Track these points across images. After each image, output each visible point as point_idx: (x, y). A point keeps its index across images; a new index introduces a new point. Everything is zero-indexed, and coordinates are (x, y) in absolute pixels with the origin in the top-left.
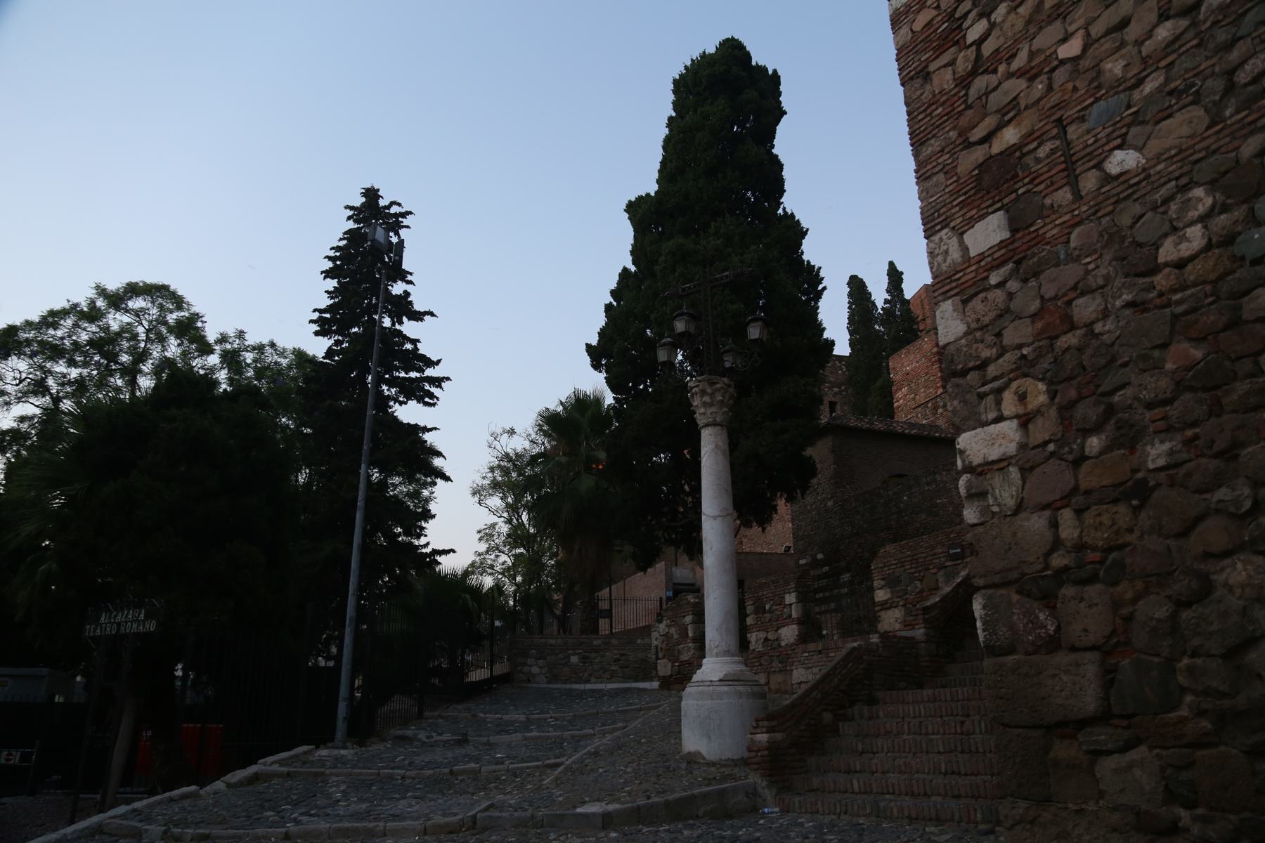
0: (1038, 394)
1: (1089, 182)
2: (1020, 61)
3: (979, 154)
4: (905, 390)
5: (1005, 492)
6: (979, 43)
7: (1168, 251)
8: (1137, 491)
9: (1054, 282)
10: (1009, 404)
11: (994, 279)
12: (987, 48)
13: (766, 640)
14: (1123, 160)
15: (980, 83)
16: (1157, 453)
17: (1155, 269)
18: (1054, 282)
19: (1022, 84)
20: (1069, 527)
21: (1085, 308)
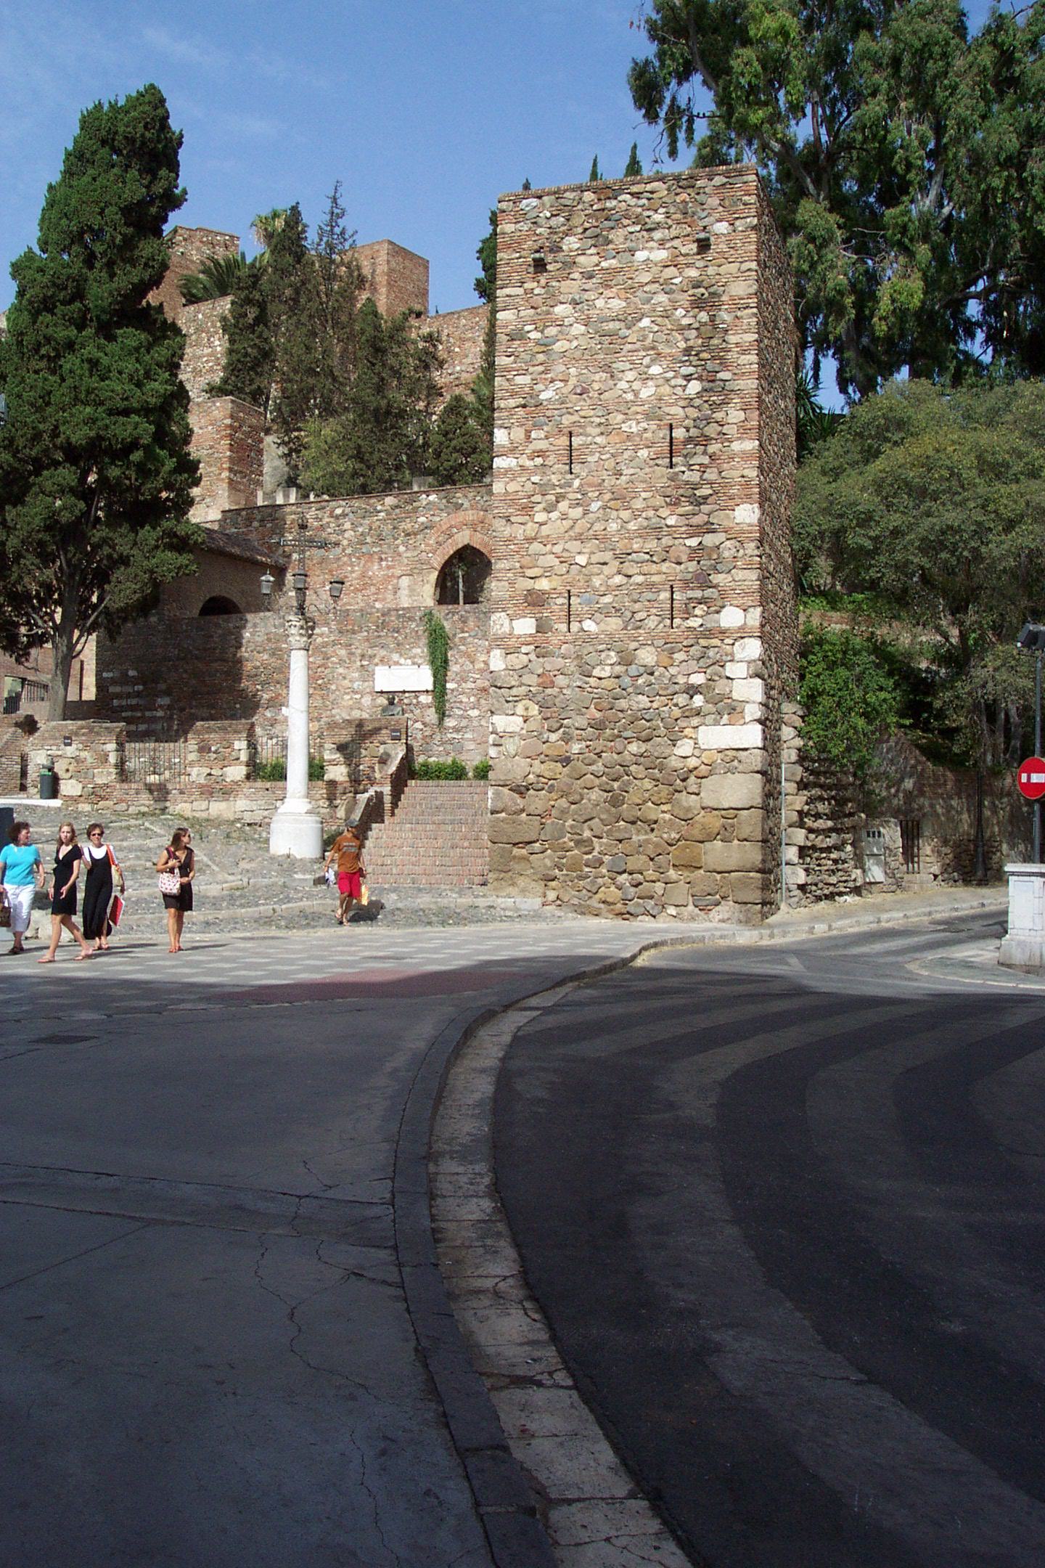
0: (534, 710)
1: (575, 626)
2: (558, 549)
3: (529, 584)
5: (511, 746)
6: (541, 524)
7: (596, 672)
8: (566, 761)
10: (520, 709)
11: (524, 649)
12: (545, 530)
13: (210, 774)
14: (589, 625)
15: (536, 547)
16: (576, 747)
20: (538, 767)
21: (561, 681)
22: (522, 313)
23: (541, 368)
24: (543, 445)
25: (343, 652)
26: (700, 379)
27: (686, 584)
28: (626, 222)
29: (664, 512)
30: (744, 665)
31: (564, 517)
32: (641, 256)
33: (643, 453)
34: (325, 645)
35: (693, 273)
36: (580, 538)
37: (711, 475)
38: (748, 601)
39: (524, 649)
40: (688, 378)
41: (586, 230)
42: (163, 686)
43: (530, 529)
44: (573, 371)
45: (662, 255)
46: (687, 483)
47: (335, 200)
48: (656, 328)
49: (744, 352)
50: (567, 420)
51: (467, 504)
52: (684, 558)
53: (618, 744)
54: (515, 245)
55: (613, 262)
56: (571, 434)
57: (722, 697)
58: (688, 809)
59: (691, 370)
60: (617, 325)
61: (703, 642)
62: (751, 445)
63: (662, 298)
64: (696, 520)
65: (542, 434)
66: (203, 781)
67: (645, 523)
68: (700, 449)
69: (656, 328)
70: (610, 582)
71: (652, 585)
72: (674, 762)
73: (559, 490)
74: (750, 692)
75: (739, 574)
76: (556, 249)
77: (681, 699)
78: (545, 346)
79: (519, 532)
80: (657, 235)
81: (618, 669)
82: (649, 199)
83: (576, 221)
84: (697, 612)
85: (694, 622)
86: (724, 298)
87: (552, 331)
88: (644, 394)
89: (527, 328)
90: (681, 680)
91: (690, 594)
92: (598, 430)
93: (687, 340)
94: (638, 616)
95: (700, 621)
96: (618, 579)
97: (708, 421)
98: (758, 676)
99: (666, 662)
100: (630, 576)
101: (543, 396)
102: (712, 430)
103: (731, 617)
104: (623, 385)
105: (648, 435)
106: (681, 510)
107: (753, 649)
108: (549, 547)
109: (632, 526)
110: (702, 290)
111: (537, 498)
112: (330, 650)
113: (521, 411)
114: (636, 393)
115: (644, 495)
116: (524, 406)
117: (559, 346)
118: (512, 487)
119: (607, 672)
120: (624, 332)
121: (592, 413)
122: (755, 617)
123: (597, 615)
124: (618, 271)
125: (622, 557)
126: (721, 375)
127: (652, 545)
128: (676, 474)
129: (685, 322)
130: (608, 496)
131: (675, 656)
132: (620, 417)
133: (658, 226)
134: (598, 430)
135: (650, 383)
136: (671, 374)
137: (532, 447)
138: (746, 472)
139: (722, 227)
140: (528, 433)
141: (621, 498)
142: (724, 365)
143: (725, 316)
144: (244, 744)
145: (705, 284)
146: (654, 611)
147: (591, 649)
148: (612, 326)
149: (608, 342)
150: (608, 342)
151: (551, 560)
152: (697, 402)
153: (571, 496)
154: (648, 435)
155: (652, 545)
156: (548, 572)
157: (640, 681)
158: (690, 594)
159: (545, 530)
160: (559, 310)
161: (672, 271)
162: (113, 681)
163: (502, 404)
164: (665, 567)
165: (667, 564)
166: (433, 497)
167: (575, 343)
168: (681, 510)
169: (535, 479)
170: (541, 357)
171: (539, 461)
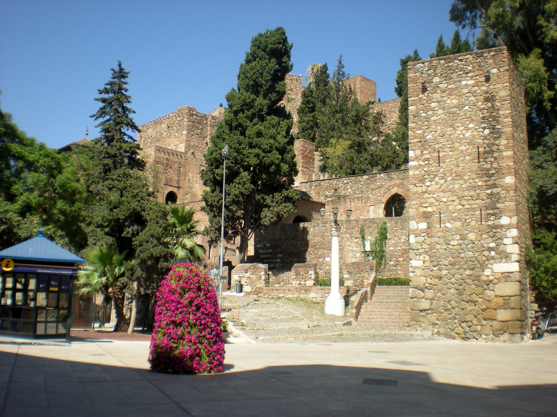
0: (427, 258)
1: (443, 225)
2: (435, 196)
3: (424, 210)
5: (418, 272)
6: (428, 186)
7: (452, 243)
8: (440, 278)
9: (433, 240)
11: (423, 235)
12: (430, 189)
13: (300, 284)
14: (448, 225)
15: (426, 195)
16: (444, 272)
17: (449, 244)
18: (433, 240)
19: (435, 201)
20: (429, 281)
22: (418, 107)
23: (426, 127)
24: (428, 156)
25: (349, 236)
26: (489, 128)
27: (487, 208)
28: (457, 70)
29: (476, 180)
30: (511, 239)
31: (437, 183)
32: (464, 83)
33: (468, 158)
35: (484, 88)
36: (443, 191)
37: (495, 165)
38: (512, 214)
39: (423, 235)
40: (484, 128)
41: (442, 74)
42: (279, 250)
43: (424, 189)
44: (439, 127)
45: (471, 82)
46: (485, 169)
47: (340, 62)
48: (471, 110)
49: (506, 117)
50: (437, 146)
52: (485, 198)
53: (461, 271)
54: (415, 81)
55: (453, 85)
56: (439, 152)
57: (503, 252)
58: (490, 297)
59: (485, 125)
60: (456, 109)
61: (494, 230)
62: (510, 153)
63: (472, 98)
64: (489, 183)
65: (427, 152)
66: (297, 286)
67: (469, 185)
68: (490, 155)
69: (471, 110)
70: (456, 208)
71: (473, 208)
72: (484, 278)
73: (435, 173)
74: (514, 250)
75: (507, 204)
76: (431, 82)
77: (486, 253)
78: (428, 119)
79: (420, 190)
80: (470, 75)
81: (460, 242)
82: (466, 62)
83: (439, 71)
84: (492, 219)
85: (490, 223)
86: (497, 97)
87: (430, 113)
88: (467, 135)
89: (421, 112)
90: (485, 245)
91: (488, 212)
92: (450, 150)
93: (483, 114)
94: (468, 221)
95: (492, 222)
96: (459, 207)
97: (493, 144)
98: (516, 243)
99: (479, 238)
100: (463, 206)
101: (427, 138)
102: (494, 148)
103: (505, 220)
104: (458, 132)
105: (469, 151)
106: (483, 179)
107: (514, 232)
108: (432, 195)
109: (464, 186)
110: (488, 95)
111: (426, 177)
113: (419, 144)
114: (464, 135)
115: (468, 174)
116: (420, 142)
117: (433, 118)
118: (417, 172)
119: (455, 243)
120: (458, 112)
121: (447, 143)
122: (514, 220)
123: (451, 221)
124: (453, 89)
125: (460, 198)
126: (497, 127)
127: (472, 193)
128: (481, 165)
129: (482, 107)
130: (454, 175)
131: (483, 236)
132: (458, 144)
133: (470, 71)
134: (450, 150)
135: (469, 131)
136: (477, 127)
137: (424, 157)
138: (509, 164)
139: (495, 71)
140: (422, 152)
141: (459, 176)
142: (498, 122)
143: (498, 104)
144: (313, 272)
145: (489, 92)
146: (474, 219)
147: (449, 234)
148: (453, 110)
149: (452, 117)
150: (452, 117)
151: (432, 200)
152: (488, 137)
153: (440, 175)
154: (469, 151)
155: (472, 193)
156: (431, 205)
157: (469, 246)
158: (488, 212)
159: (430, 189)
160: (433, 105)
161: (476, 88)
162: (261, 248)
163: (412, 141)
164: (477, 201)
165: (479, 200)
166: (382, 175)
167: (439, 117)
168: (483, 179)
169: (425, 169)
170: (426, 123)
171: (427, 162)
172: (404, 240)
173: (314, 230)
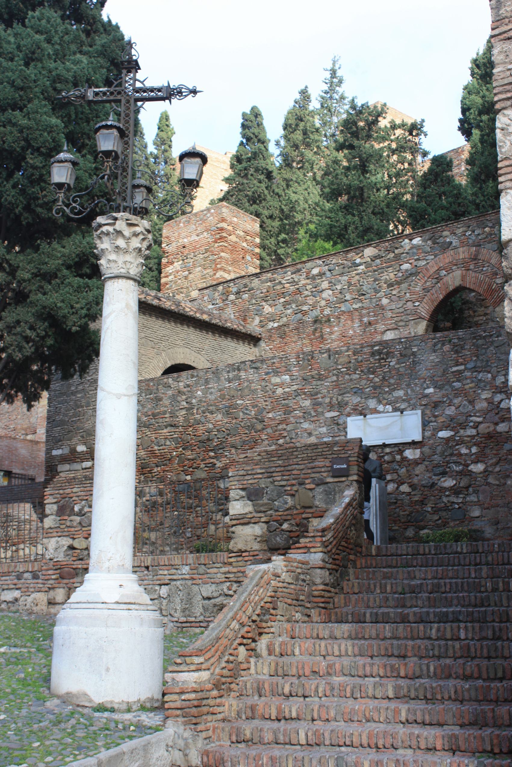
4: (177, 265)
13: (71, 548)
34: (287, 396)
51: (455, 242)
66: (61, 557)
112: (291, 403)
166: (417, 241)
172: (485, 404)
173: (205, 392)
